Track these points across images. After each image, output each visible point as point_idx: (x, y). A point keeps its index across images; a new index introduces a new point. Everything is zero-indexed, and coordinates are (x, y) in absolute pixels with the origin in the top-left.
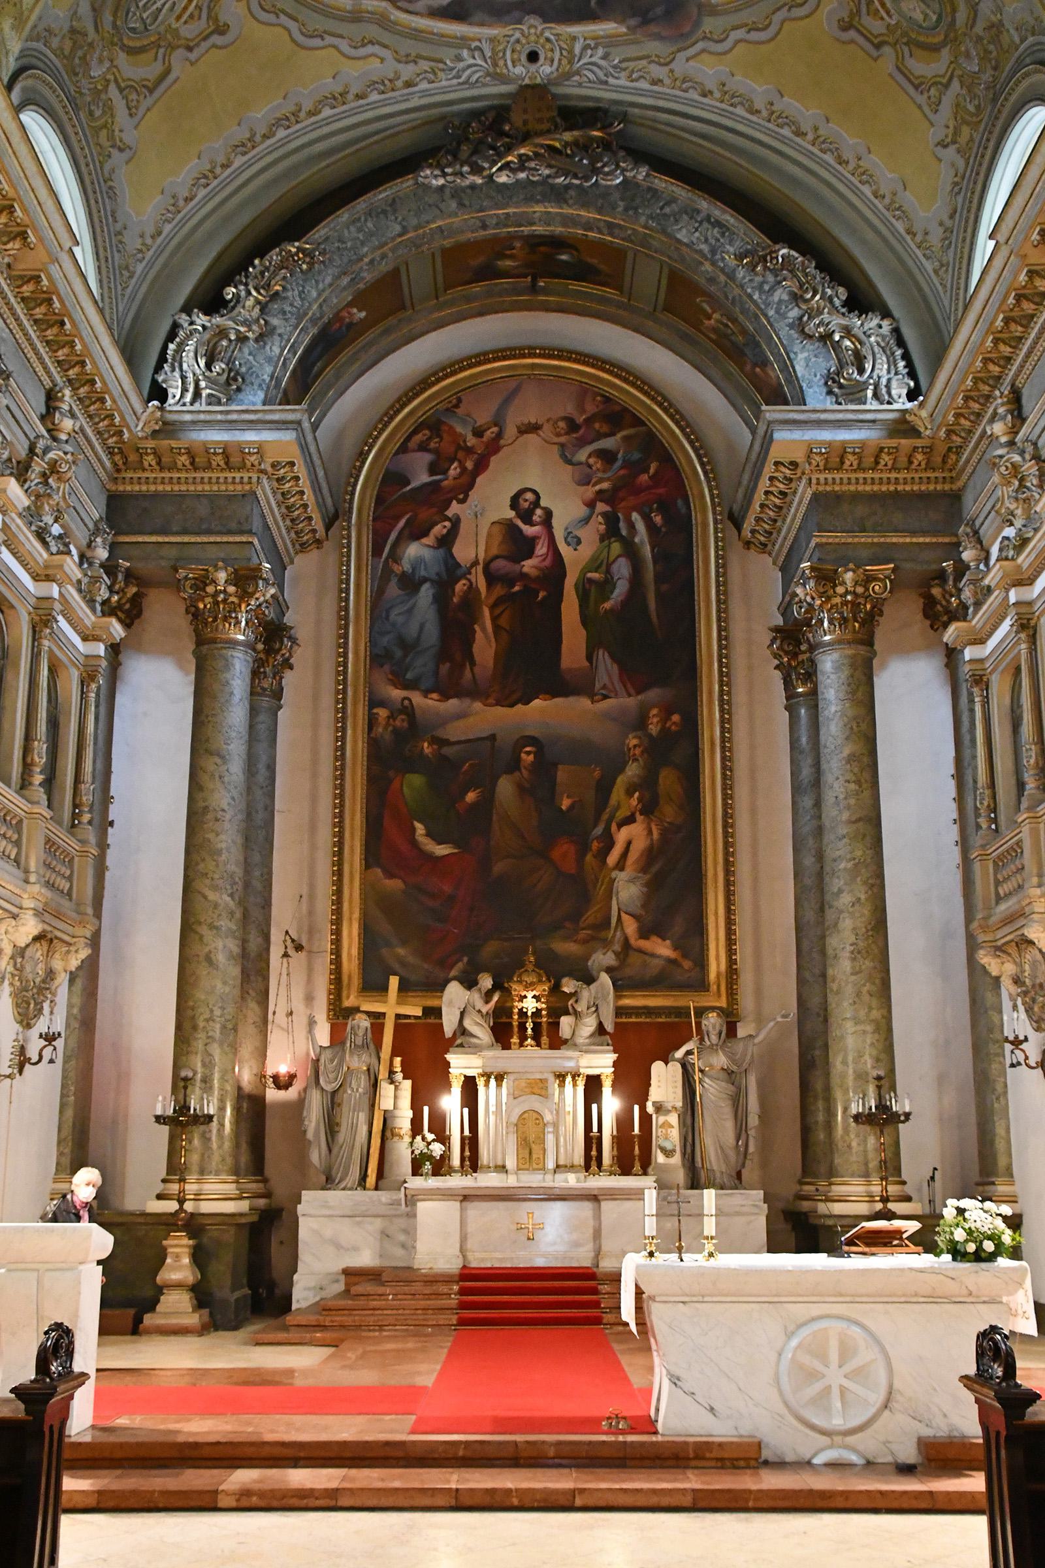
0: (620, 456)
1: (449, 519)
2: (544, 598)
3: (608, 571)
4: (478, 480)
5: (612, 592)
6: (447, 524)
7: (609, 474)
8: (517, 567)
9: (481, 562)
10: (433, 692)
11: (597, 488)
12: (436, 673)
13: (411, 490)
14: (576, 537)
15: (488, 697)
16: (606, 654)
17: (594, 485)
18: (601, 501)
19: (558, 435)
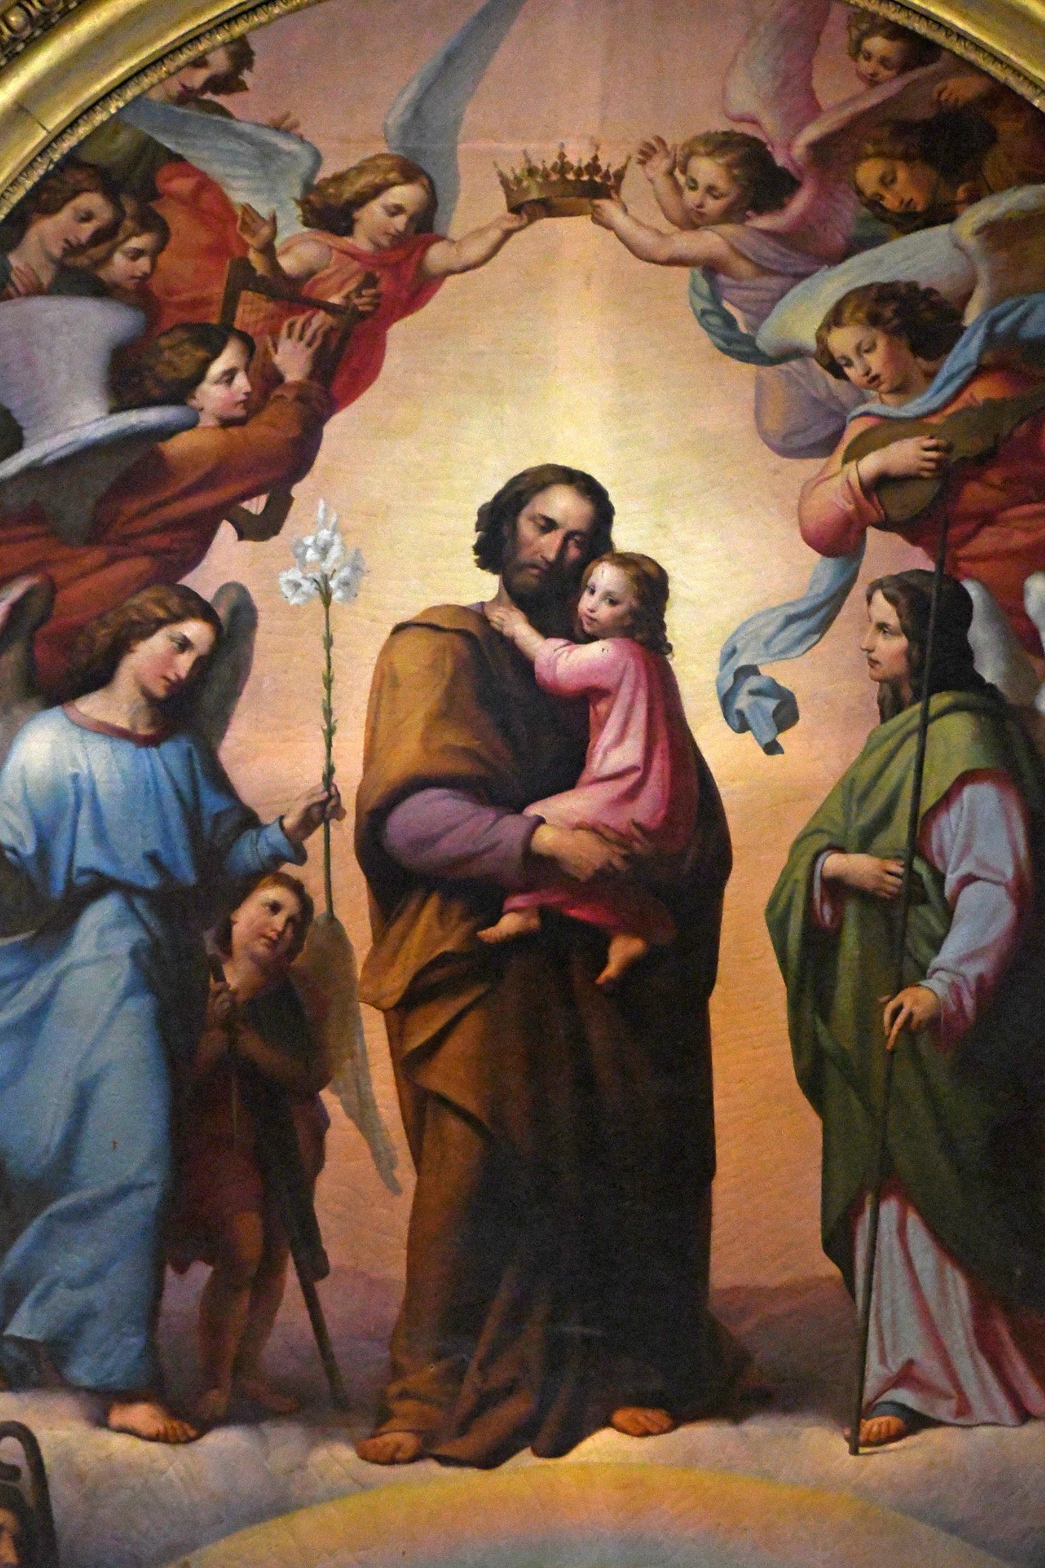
0: (973, 313)
1: (206, 612)
2: (633, 967)
3: (918, 845)
4: (336, 428)
5: (936, 945)
6: (195, 630)
7: (913, 407)
8: (511, 828)
9: (349, 802)
10: (129, 1397)
11: (871, 464)
12: (152, 1314)
13: (32, 471)
14: (774, 690)
15: (383, 1417)
16: (913, 1219)
17: (855, 453)
18: (885, 525)
19: (692, 221)
